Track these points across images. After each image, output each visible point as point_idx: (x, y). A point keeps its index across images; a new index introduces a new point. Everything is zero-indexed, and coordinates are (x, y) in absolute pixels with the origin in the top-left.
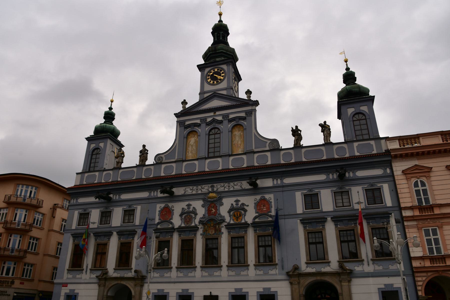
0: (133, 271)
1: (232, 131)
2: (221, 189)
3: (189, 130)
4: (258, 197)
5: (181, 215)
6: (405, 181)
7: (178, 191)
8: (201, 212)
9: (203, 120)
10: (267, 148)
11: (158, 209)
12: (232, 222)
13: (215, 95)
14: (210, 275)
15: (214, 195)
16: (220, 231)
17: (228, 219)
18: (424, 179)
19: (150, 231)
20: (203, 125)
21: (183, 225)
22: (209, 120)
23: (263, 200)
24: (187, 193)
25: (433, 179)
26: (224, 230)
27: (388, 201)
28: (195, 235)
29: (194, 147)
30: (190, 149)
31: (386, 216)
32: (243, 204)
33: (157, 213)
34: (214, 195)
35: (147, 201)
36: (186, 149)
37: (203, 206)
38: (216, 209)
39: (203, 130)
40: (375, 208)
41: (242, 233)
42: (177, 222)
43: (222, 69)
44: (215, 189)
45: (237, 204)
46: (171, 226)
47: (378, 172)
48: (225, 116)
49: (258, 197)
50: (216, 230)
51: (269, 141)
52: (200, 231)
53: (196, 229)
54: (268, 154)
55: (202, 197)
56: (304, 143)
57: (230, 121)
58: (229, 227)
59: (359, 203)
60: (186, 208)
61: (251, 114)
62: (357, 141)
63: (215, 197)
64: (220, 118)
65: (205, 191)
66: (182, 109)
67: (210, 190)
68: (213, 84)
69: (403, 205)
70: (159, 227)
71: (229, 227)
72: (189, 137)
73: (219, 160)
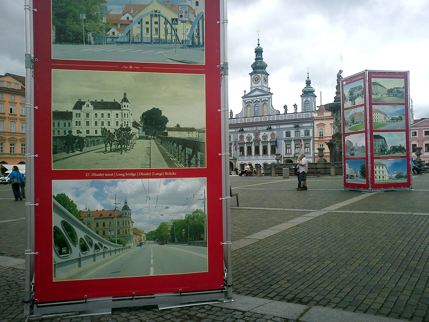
0: (233, 157)
1: (263, 106)
2: (260, 129)
3: (247, 104)
4: (272, 132)
5: (247, 138)
6: (317, 128)
7: (245, 129)
8: (253, 137)
9: (253, 100)
10: (275, 114)
11: (239, 136)
12: (263, 141)
13: (257, 89)
14: (257, 158)
15: (257, 131)
16: (259, 144)
17: (262, 140)
18: (323, 128)
19: (237, 143)
20: (253, 103)
21: (248, 142)
22: (255, 100)
23: (273, 134)
24: (248, 130)
25: (325, 128)
26: (261, 143)
27: (311, 135)
28: (252, 145)
29: (250, 112)
30: (248, 112)
31: (310, 140)
32: (267, 135)
33: (239, 137)
34: (257, 131)
35: (235, 133)
36: (247, 112)
37: (254, 135)
38: (258, 136)
39: (252, 105)
40: (307, 137)
41: (266, 145)
42: (245, 140)
43: (259, 76)
44: (258, 129)
45: (265, 135)
46: (243, 142)
47: (309, 125)
48: (261, 99)
49: (272, 132)
50: (258, 144)
51: (276, 111)
52: (253, 144)
53: (252, 143)
54: (275, 116)
55: (253, 132)
56: (288, 112)
57: (262, 101)
58: (262, 142)
59: (302, 135)
60: (248, 135)
61: (270, 98)
62: (305, 112)
63: (257, 132)
64: (259, 100)
65: (254, 129)
66: (244, 95)
67: (256, 129)
68: (256, 83)
69: (315, 137)
70: (240, 142)
71: (262, 142)
72: (248, 107)
73: (259, 117)
